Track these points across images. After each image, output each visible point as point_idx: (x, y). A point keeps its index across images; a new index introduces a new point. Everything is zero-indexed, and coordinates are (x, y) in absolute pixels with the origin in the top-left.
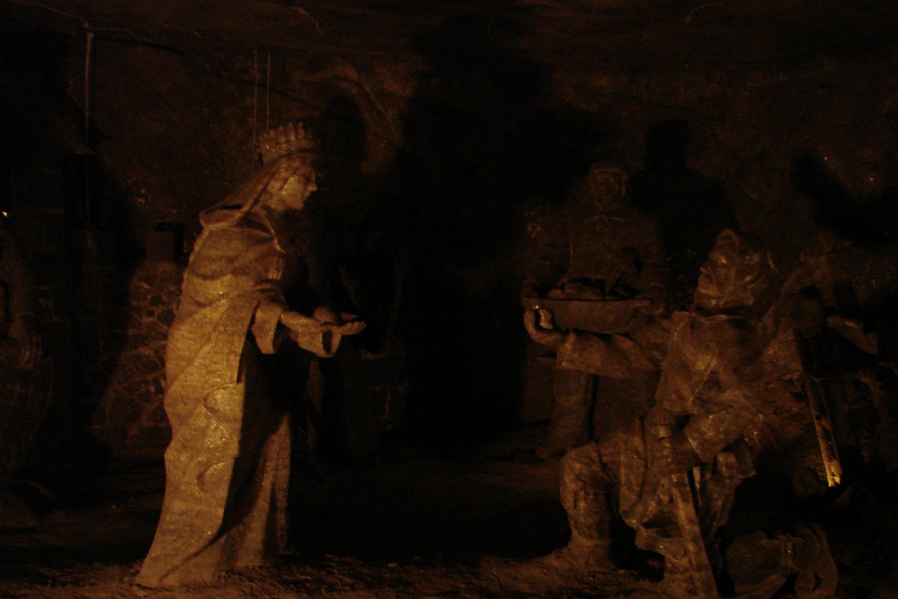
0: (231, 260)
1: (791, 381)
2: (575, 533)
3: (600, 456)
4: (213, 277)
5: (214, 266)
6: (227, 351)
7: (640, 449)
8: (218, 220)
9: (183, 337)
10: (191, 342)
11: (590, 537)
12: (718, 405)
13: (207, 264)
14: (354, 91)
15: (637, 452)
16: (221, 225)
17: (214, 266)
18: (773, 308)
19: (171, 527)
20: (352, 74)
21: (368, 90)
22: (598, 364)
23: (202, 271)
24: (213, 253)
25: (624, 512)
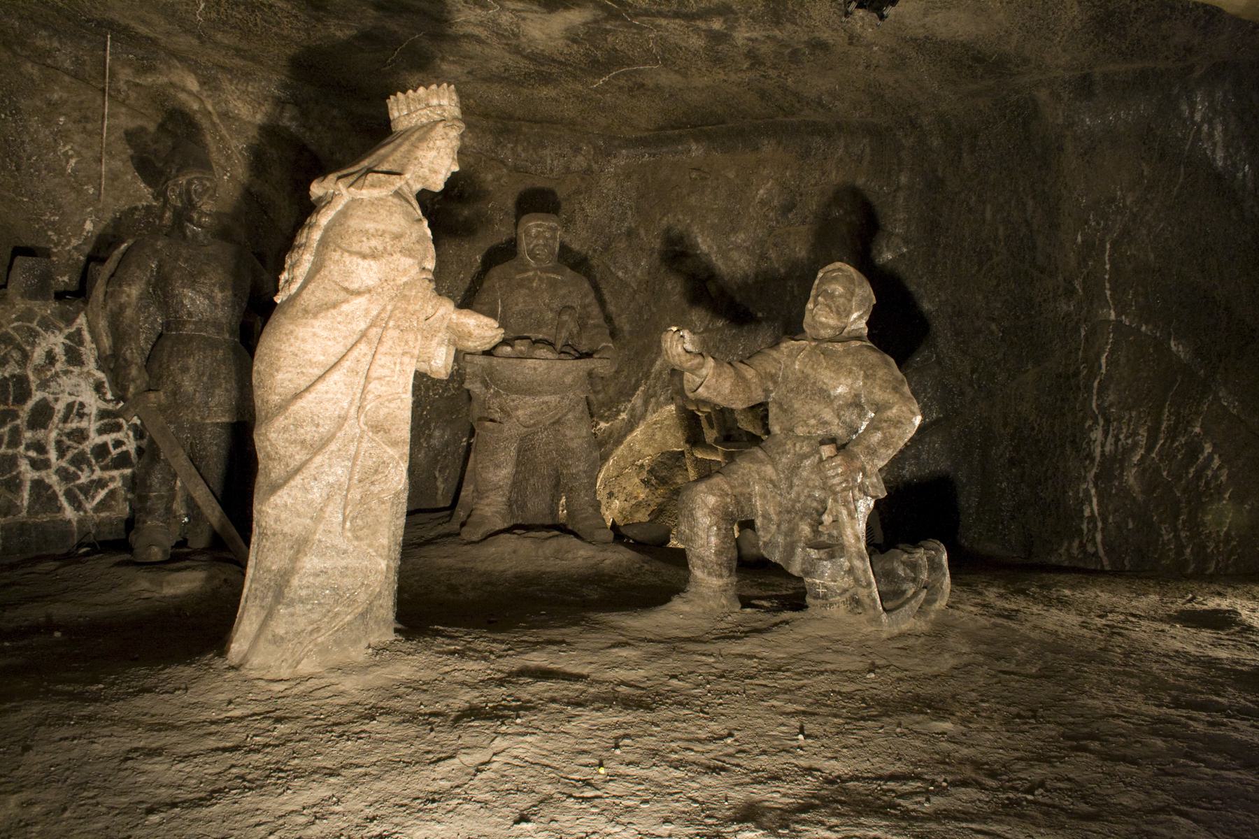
0: (397, 237)
1: (642, 466)
2: (698, 573)
3: (732, 487)
4: (373, 255)
5: (373, 243)
6: (399, 351)
7: (774, 478)
8: (373, 186)
9: (314, 334)
10: (329, 343)
11: (721, 576)
12: (886, 421)
13: (364, 239)
14: (196, 106)
15: (771, 481)
16: (377, 193)
17: (373, 243)
18: (642, 388)
19: (303, 593)
20: (192, 84)
21: (210, 108)
22: (727, 391)
23: (356, 248)
24: (370, 226)
25: (766, 544)
